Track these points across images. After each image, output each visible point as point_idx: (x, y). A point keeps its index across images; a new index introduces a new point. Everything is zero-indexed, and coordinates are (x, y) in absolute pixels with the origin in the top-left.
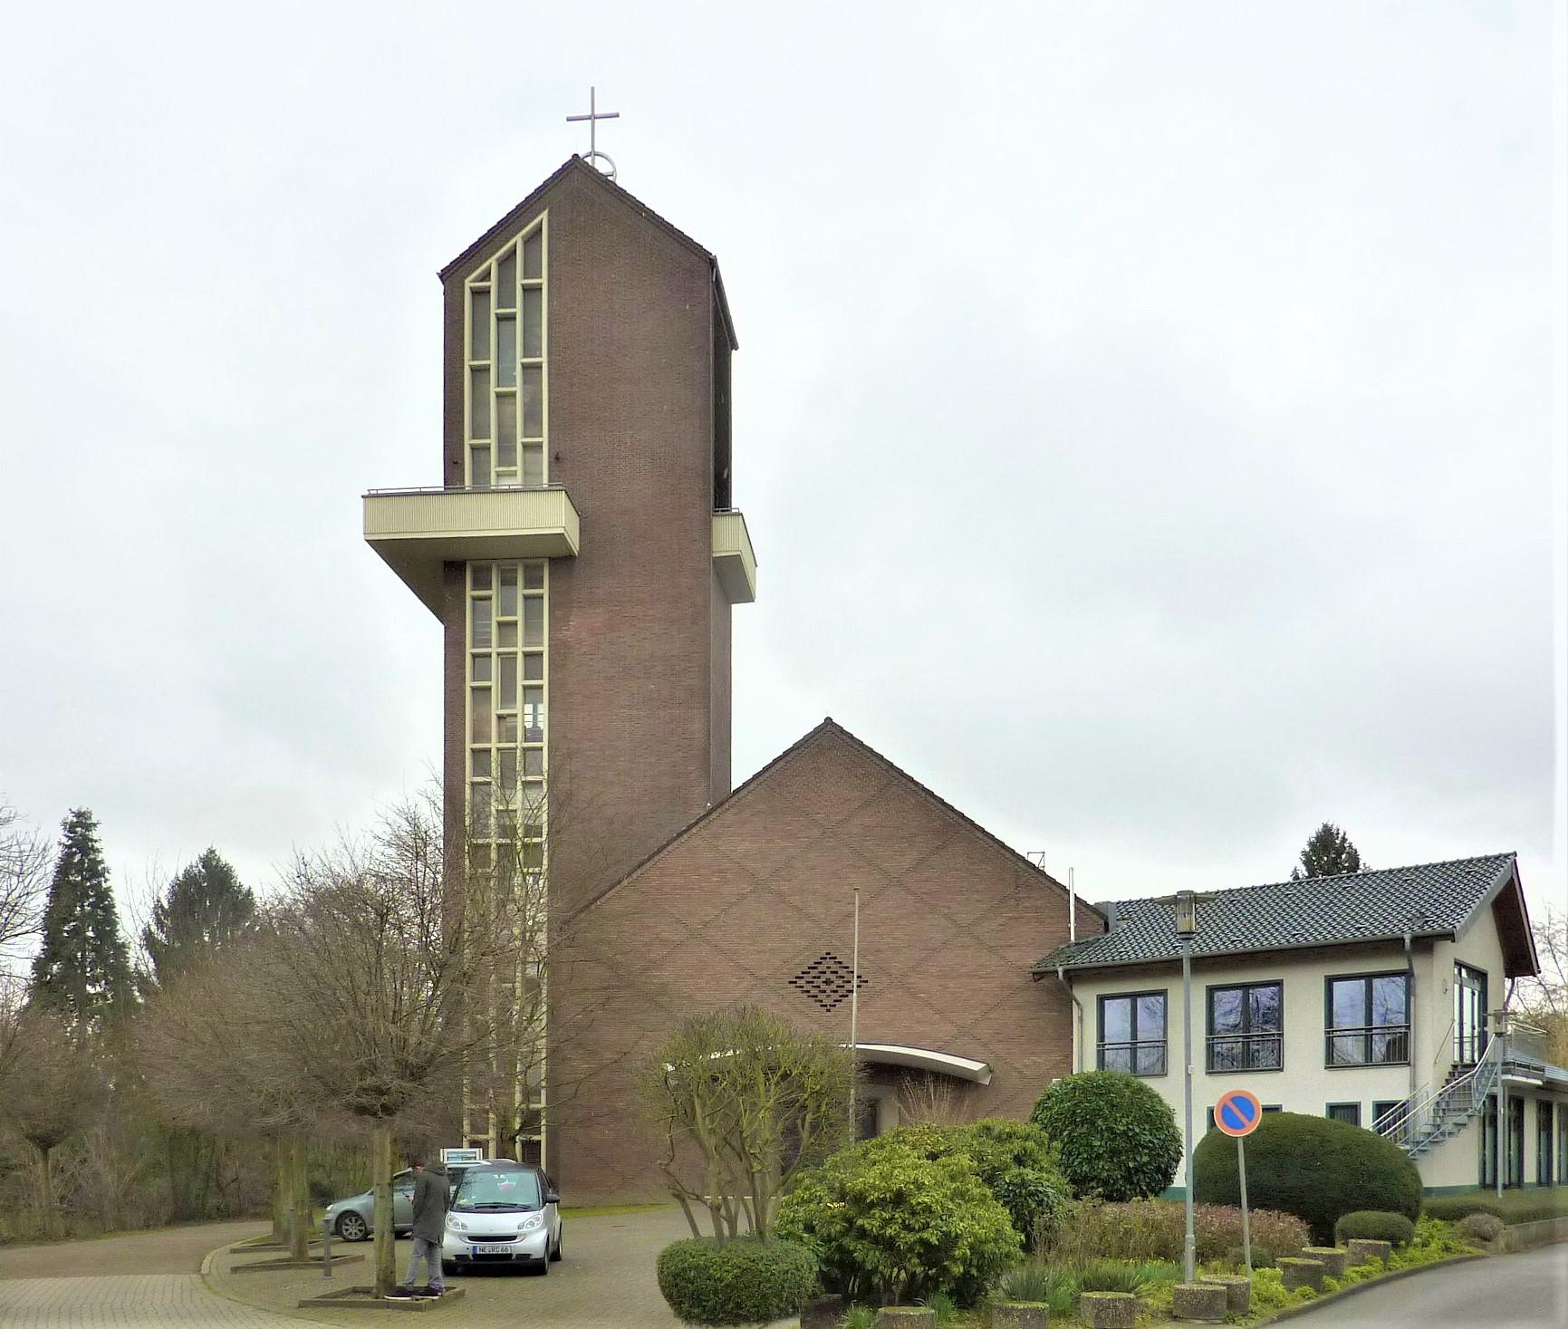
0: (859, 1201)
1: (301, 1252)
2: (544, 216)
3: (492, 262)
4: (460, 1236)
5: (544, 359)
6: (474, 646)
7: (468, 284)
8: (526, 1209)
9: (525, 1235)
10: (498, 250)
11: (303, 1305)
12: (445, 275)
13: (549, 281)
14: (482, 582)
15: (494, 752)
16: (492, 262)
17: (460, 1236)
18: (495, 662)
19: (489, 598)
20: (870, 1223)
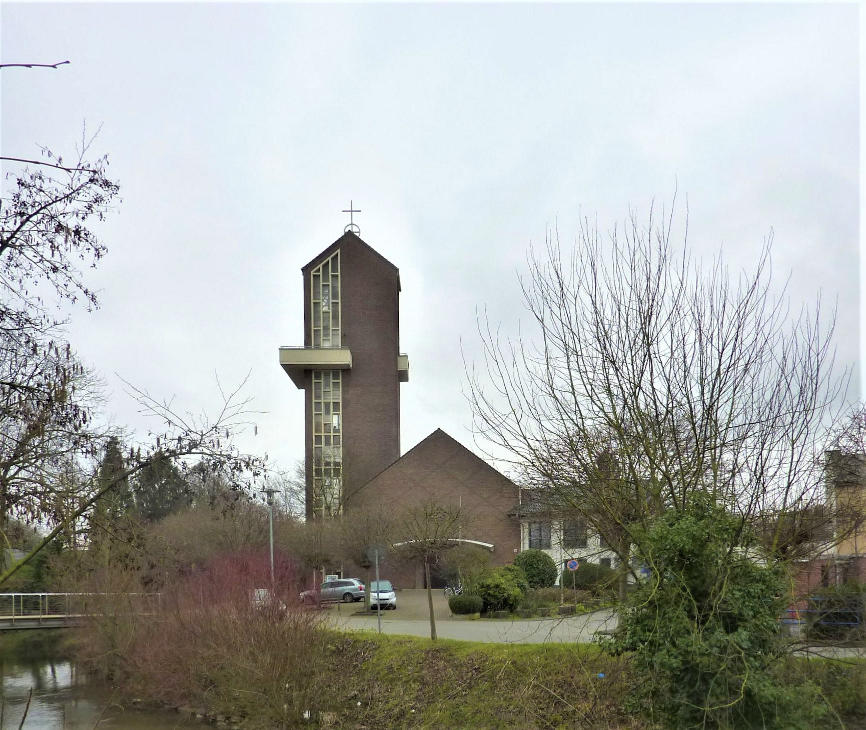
0: (488, 587)
1: (320, 607)
2: (339, 251)
3: (321, 266)
4: (374, 599)
5: (339, 301)
6: (315, 399)
7: (312, 273)
8: (389, 592)
9: (391, 599)
10: (322, 261)
11: (352, 615)
12: (303, 269)
13: (341, 274)
14: (318, 377)
15: (323, 437)
16: (321, 266)
17: (374, 599)
18: (323, 405)
19: (321, 383)
20: (491, 592)
